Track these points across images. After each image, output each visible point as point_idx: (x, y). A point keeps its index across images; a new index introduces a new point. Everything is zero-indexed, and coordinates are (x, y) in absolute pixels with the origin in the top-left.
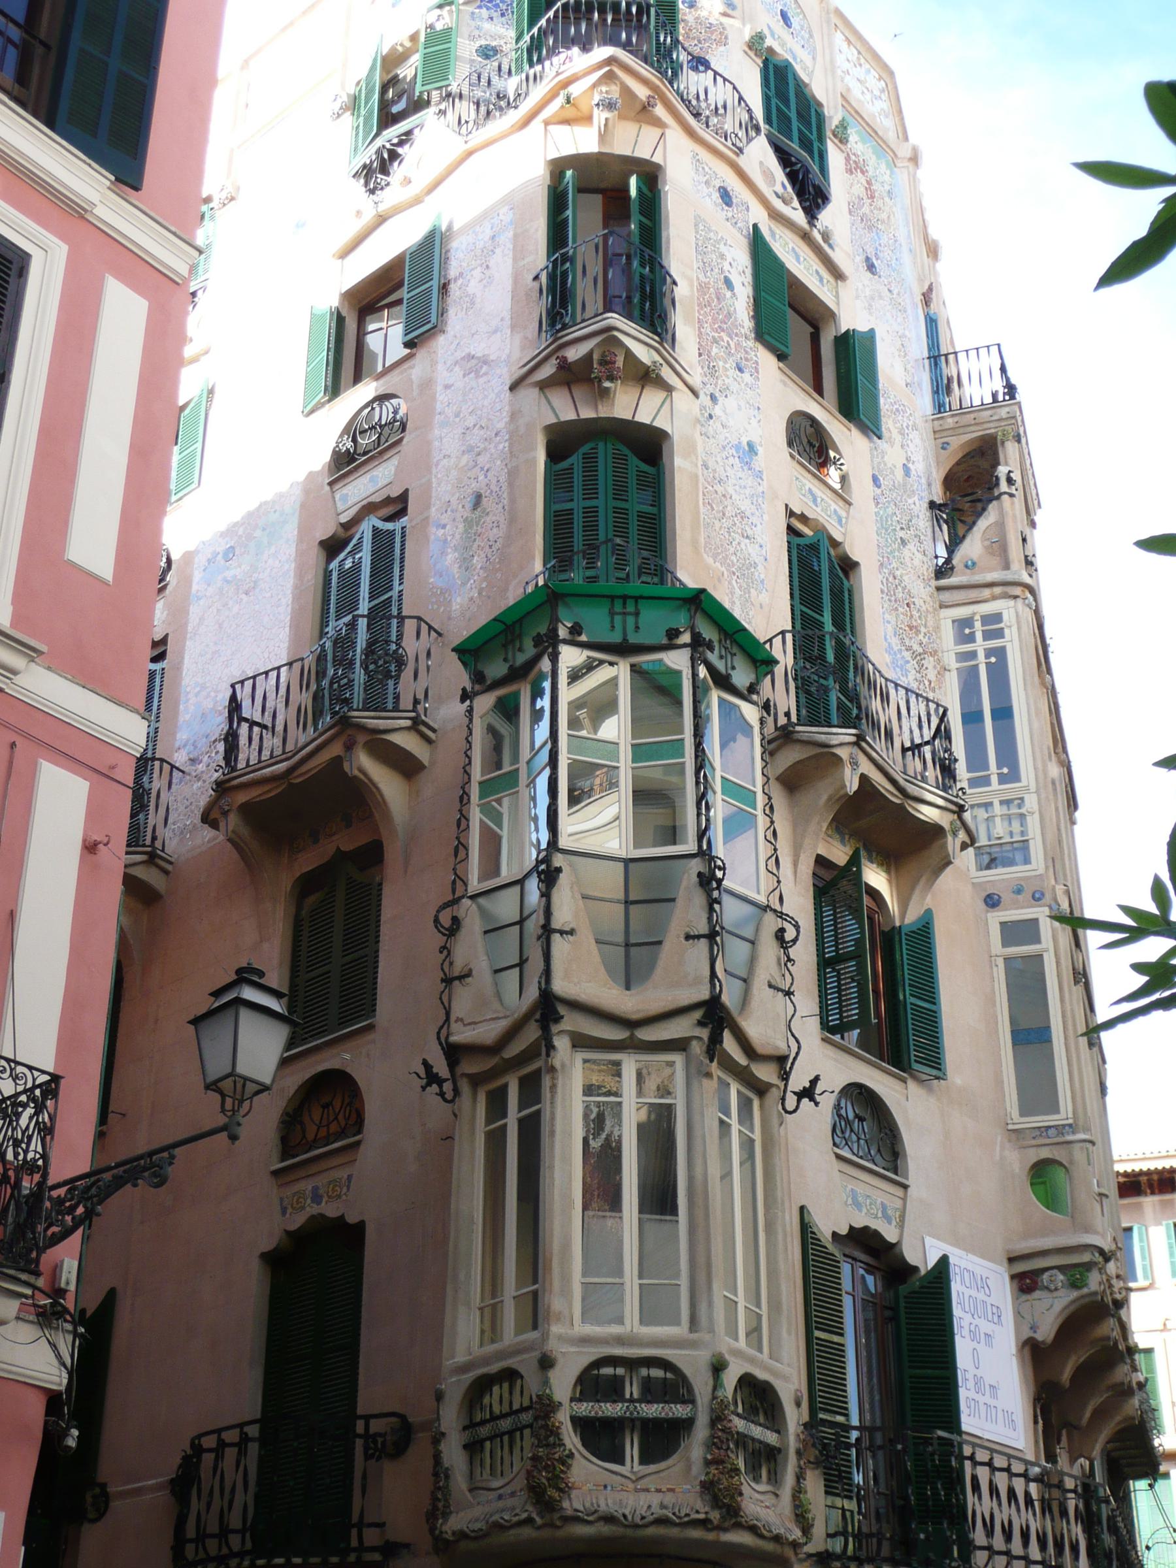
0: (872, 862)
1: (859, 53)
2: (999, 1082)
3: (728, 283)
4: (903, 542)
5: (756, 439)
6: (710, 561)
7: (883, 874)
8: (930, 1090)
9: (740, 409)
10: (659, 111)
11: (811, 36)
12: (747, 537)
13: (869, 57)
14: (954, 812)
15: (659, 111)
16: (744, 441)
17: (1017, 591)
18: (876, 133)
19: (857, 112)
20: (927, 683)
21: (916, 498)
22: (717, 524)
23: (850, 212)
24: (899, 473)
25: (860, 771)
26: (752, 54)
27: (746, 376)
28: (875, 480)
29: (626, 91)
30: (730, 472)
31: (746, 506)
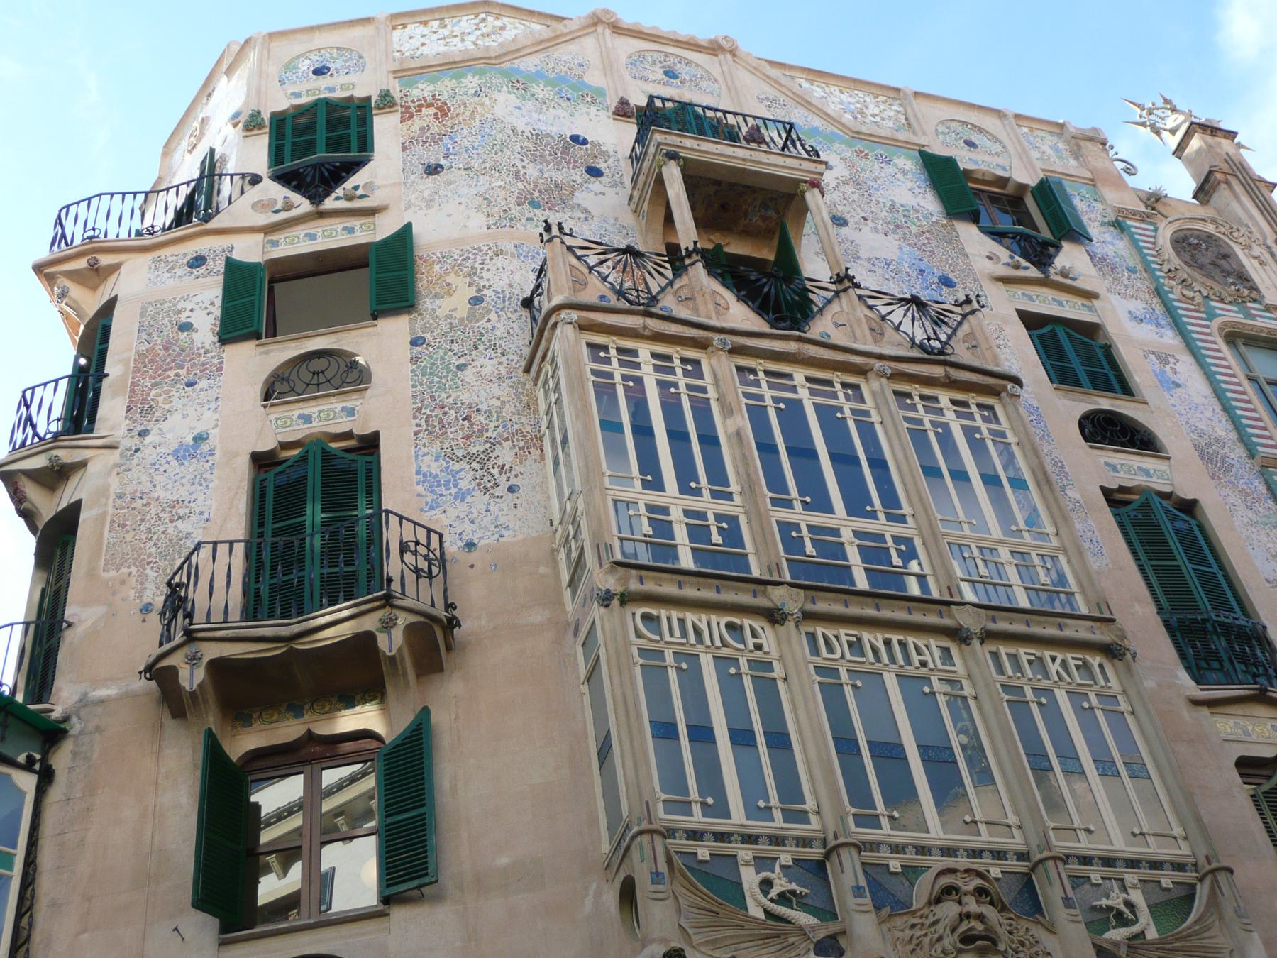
0: (353, 706)
1: (441, 19)
2: (594, 821)
3: (186, 327)
4: (460, 368)
5: (200, 428)
6: (113, 573)
7: (375, 707)
8: (438, 898)
9: (185, 416)
10: (105, 260)
11: (360, 57)
12: (180, 518)
13: (454, 14)
14: (383, 607)
15: (105, 260)
16: (189, 440)
17: (552, 321)
18: (455, 63)
19: (422, 68)
20: (495, 472)
21: (493, 316)
22: (129, 537)
23: (404, 149)
24: (463, 309)
25: (206, 660)
26: (256, 132)
27: (203, 383)
28: (415, 343)
29: (70, 275)
30: (158, 478)
31: (183, 493)
